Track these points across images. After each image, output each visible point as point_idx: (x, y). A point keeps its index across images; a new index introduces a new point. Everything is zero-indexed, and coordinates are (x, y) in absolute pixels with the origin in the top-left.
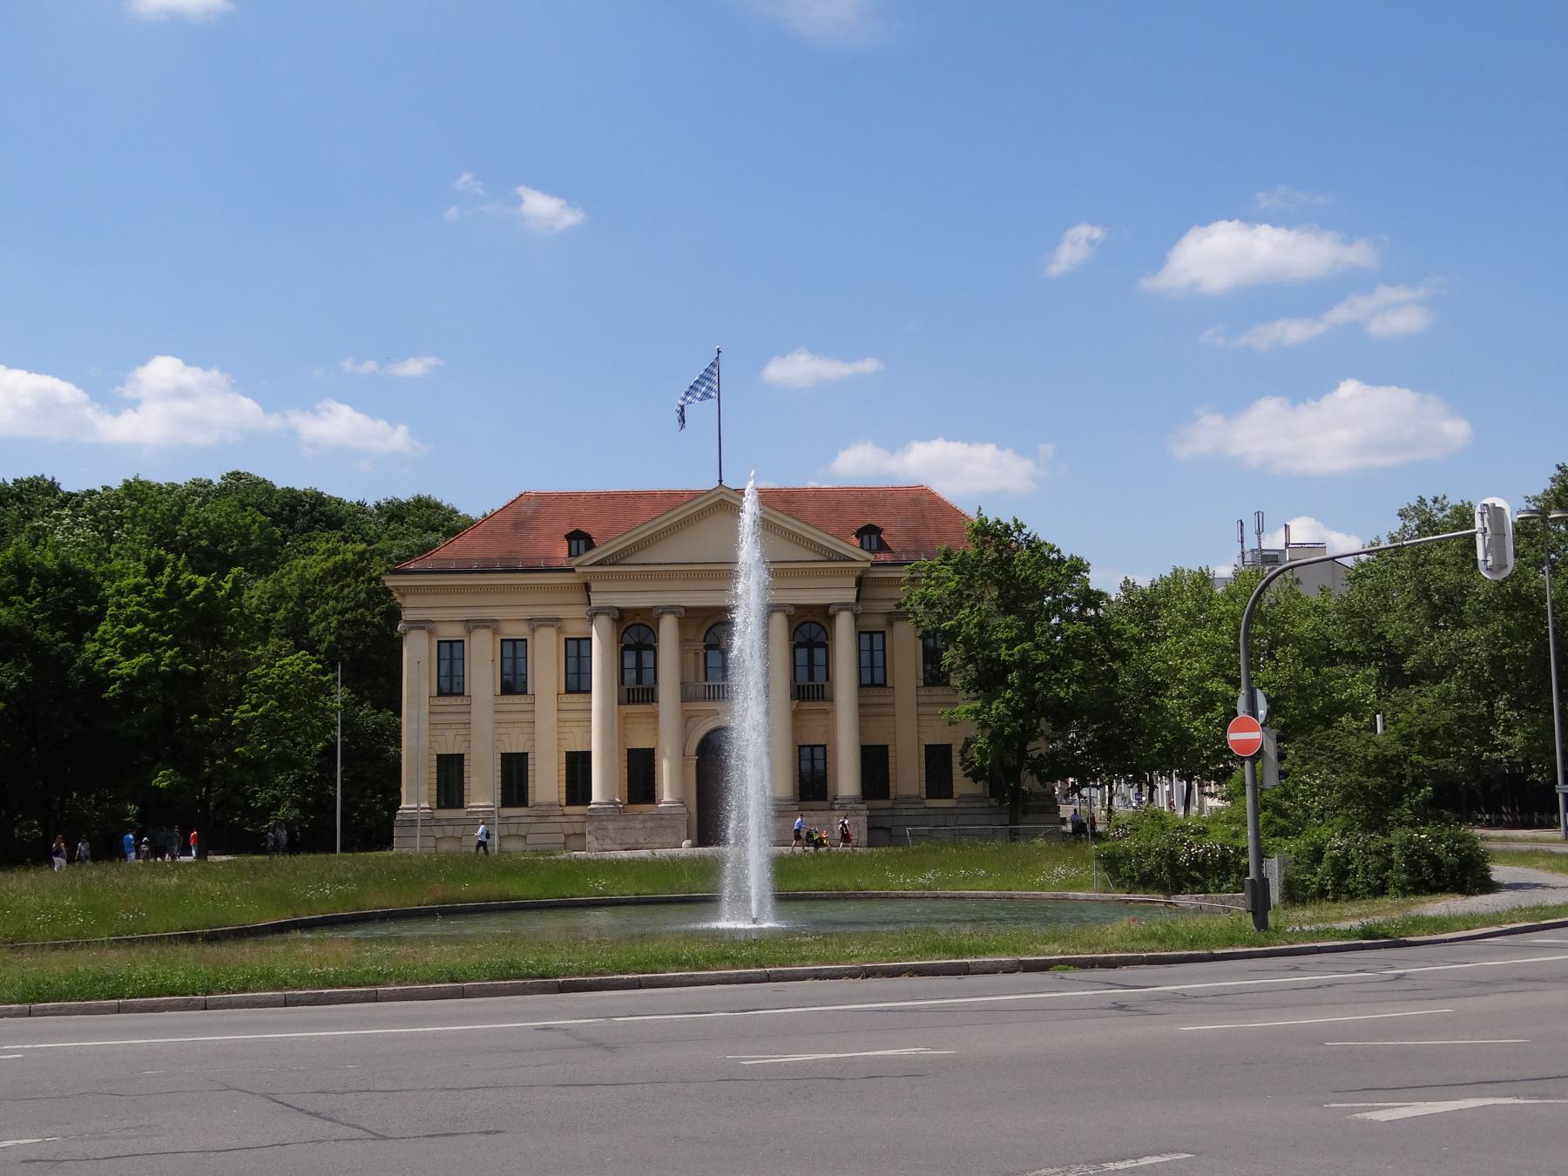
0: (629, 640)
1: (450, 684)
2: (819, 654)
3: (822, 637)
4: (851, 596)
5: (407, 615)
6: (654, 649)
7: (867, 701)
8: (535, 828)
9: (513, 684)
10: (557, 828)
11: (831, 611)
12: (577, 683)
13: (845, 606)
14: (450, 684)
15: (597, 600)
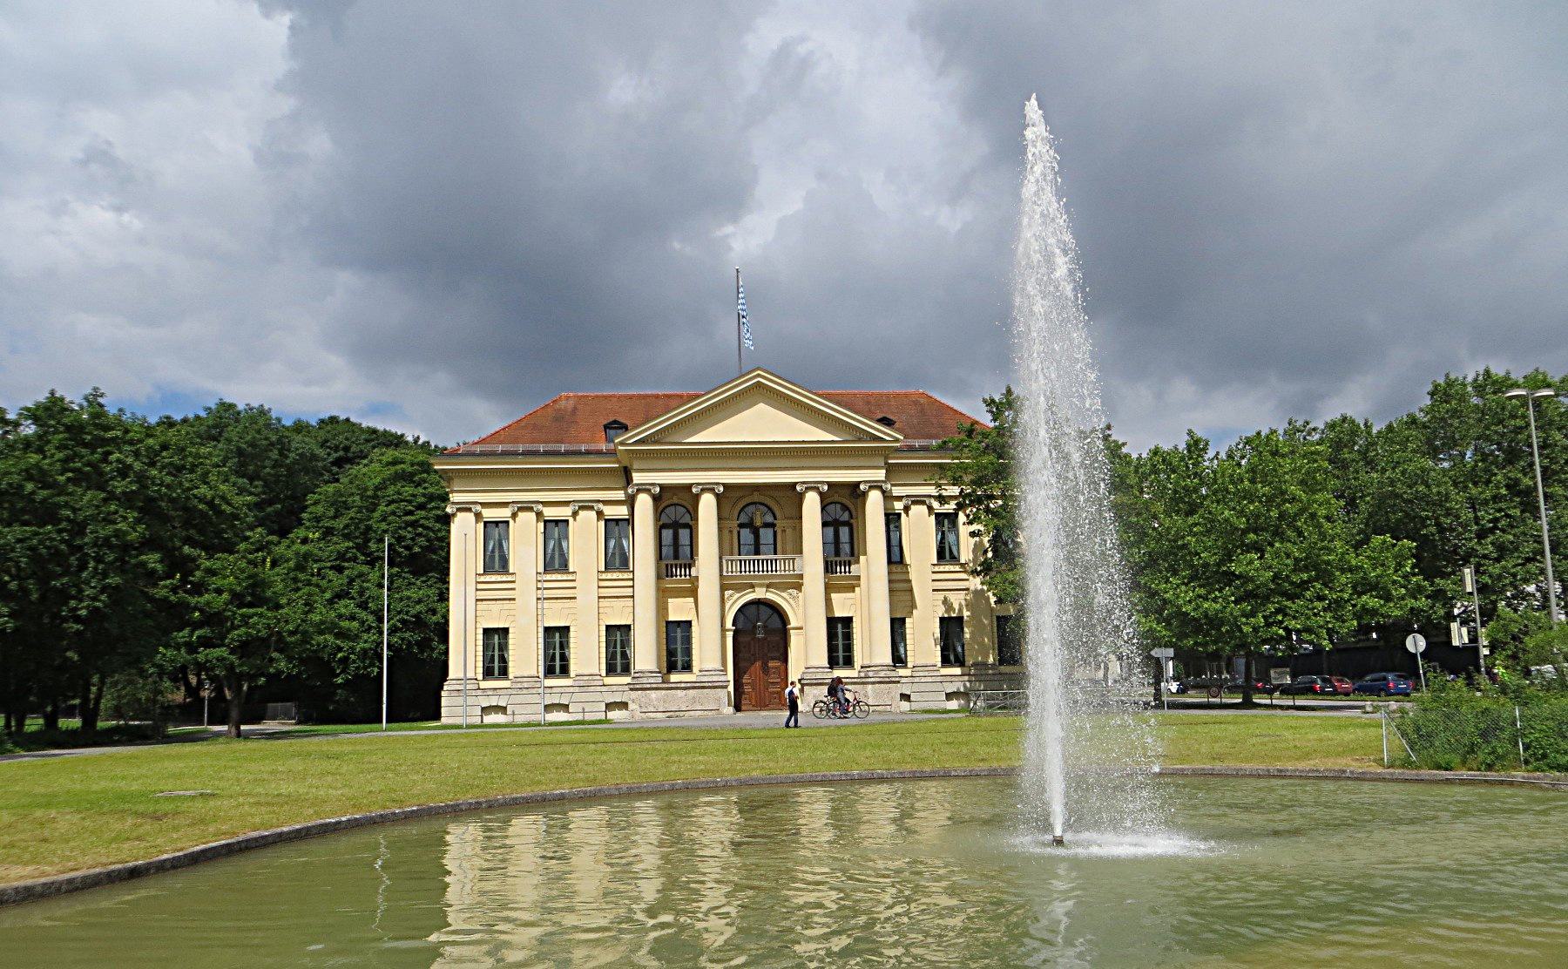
0: (664, 519)
1: (496, 561)
2: (844, 532)
3: (846, 517)
4: (880, 475)
5: (454, 497)
6: (692, 529)
7: (894, 577)
8: (576, 697)
9: (556, 561)
10: (598, 697)
11: (862, 487)
12: (618, 560)
13: (875, 485)
14: (496, 561)
15: (638, 478)
